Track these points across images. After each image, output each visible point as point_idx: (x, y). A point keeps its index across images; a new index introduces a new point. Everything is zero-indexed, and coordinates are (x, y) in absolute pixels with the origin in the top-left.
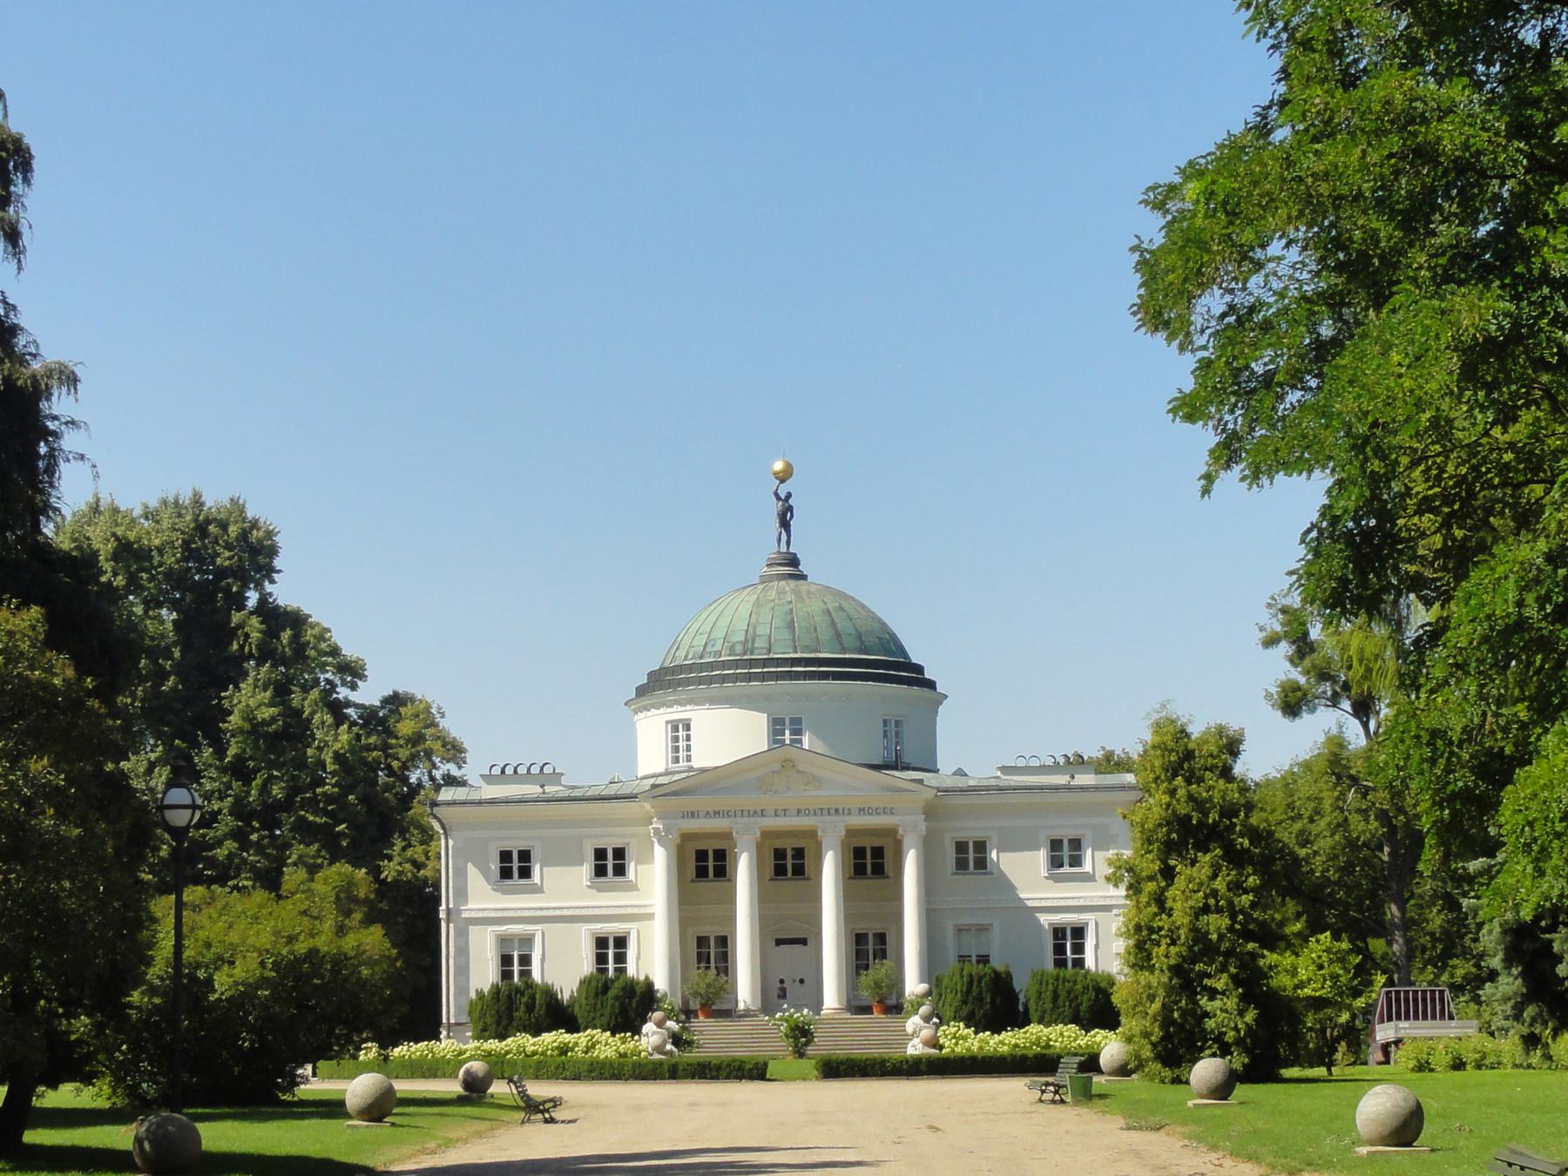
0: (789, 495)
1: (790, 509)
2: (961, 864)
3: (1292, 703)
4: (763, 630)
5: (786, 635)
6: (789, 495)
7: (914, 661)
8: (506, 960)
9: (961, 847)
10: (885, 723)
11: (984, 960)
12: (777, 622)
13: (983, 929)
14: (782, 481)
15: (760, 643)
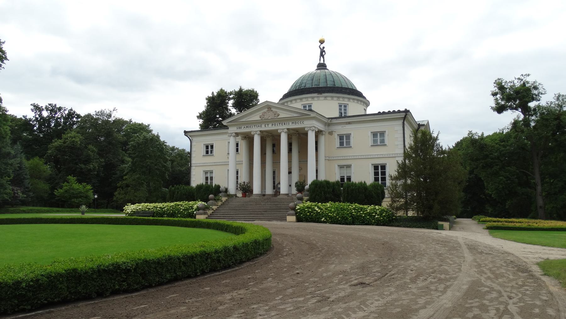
0: (324, 48)
1: (324, 51)
2: (342, 144)
3: (500, 109)
4: (304, 82)
5: (310, 82)
6: (324, 48)
7: (358, 90)
8: (207, 178)
9: (341, 137)
10: (340, 106)
11: (349, 179)
12: (309, 79)
13: (349, 166)
14: (322, 44)
15: (303, 85)
